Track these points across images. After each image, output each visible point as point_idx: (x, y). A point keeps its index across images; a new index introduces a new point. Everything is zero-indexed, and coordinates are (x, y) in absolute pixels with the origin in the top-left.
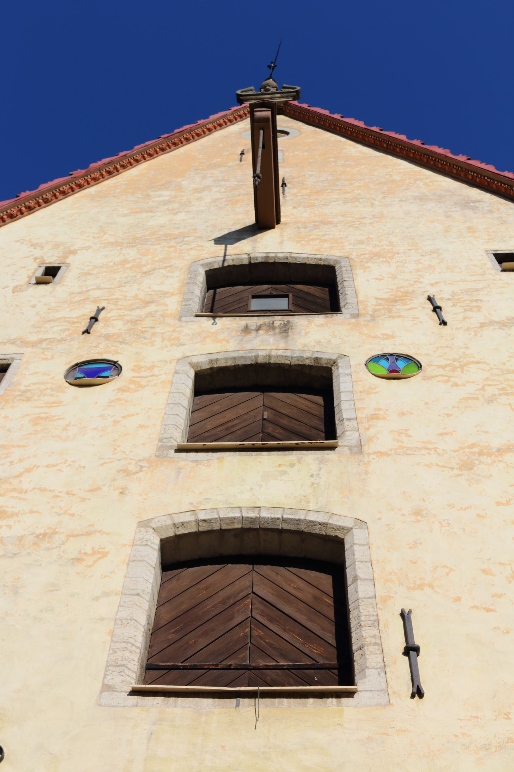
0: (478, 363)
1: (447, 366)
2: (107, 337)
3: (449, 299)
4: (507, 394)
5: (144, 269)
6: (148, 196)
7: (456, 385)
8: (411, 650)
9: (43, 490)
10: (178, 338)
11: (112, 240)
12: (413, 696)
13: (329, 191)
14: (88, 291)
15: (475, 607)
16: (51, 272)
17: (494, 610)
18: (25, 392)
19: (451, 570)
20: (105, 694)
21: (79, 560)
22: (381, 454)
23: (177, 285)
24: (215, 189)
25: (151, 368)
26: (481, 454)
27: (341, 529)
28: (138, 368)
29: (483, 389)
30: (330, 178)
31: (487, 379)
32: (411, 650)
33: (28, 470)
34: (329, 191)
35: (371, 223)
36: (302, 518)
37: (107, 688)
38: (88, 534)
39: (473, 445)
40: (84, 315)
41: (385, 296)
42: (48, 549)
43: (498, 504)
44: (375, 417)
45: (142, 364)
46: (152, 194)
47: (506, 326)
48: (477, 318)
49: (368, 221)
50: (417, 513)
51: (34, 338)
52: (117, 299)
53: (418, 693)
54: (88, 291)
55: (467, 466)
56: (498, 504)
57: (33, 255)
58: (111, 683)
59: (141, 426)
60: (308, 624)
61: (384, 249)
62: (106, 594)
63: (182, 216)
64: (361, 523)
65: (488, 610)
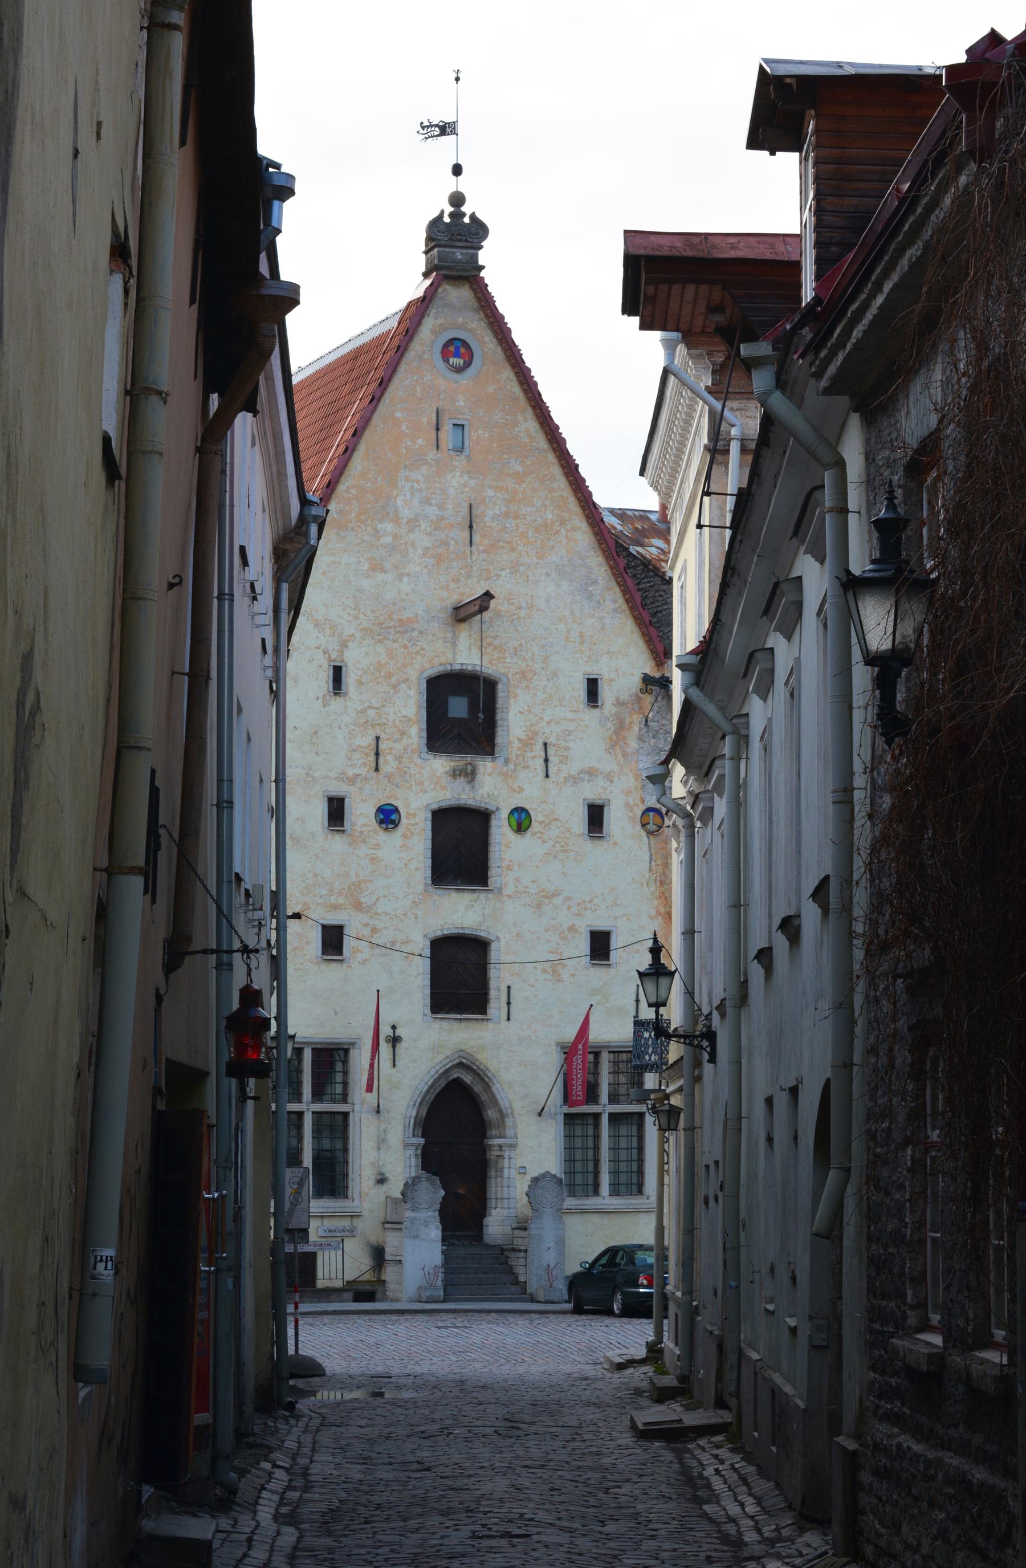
0: (556, 820)
1: (543, 821)
2: (389, 777)
3: (554, 745)
4: (563, 851)
5: (394, 680)
6: (376, 530)
7: (544, 842)
8: (509, 1003)
9: (386, 913)
10: (422, 784)
11: (365, 625)
13: (501, 544)
14: (366, 710)
16: (338, 673)
18: (361, 832)
22: (509, 896)
23: (414, 710)
24: (423, 526)
25: (415, 815)
26: (545, 897)
28: (408, 816)
29: (554, 846)
30: (504, 509)
31: (558, 836)
32: (509, 1003)
33: (378, 900)
34: (501, 544)
35: (524, 618)
37: (425, 1015)
38: (408, 942)
39: (543, 890)
40: (370, 745)
41: (523, 737)
44: (509, 868)
45: (410, 811)
46: (379, 526)
47: (575, 782)
48: (564, 774)
49: (523, 613)
50: (518, 935)
51: (351, 773)
52: (385, 724)
53: (509, 1019)
54: (366, 710)
55: (539, 906)
57: (321, 645)
59: (417, 869)
61: (528, 665)
63: (406, 586)
64: (498, 938)
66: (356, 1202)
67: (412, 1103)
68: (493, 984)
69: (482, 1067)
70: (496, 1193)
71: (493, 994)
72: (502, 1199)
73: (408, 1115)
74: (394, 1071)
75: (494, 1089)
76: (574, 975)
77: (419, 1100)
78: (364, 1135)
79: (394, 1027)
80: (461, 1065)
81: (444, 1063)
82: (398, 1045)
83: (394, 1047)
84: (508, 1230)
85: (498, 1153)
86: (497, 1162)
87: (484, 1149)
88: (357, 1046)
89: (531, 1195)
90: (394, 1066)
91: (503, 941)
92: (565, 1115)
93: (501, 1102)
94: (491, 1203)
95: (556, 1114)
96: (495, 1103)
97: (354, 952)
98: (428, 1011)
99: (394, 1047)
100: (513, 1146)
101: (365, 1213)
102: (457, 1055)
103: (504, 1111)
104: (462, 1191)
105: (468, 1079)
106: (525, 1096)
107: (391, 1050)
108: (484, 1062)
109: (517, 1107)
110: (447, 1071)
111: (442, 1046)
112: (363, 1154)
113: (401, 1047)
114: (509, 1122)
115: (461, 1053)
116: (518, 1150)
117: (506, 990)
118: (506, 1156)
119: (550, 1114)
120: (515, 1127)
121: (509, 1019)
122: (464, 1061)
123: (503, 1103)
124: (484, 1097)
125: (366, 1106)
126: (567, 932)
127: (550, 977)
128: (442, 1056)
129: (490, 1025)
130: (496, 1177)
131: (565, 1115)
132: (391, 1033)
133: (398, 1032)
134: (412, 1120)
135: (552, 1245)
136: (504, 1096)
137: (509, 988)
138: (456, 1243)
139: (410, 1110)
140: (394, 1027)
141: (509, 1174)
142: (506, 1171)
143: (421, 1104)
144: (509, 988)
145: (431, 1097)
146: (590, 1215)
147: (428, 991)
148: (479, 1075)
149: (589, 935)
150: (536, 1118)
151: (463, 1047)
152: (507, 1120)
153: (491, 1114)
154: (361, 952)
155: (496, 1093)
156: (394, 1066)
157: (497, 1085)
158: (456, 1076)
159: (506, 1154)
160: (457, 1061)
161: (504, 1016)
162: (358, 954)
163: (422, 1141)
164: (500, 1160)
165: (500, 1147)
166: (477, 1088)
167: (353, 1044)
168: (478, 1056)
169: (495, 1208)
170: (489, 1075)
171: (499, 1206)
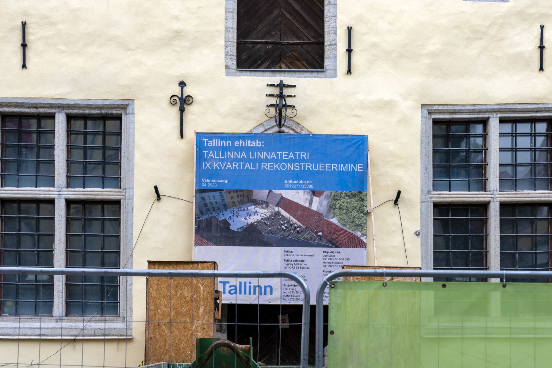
8: (349, 51)
32: (349, 51)
53: (349, 72)
79: (182, 84)
83: (182, 110)
88: (129, 110)
92: (436, 205)
99: (182, 110)
121: (349, 72)
131: (436, 205)
132: (177, 90)
133: (188, 91)
137: (350, 30)
140: (182, 84)
144: (350, 30)
167: (125, 107)
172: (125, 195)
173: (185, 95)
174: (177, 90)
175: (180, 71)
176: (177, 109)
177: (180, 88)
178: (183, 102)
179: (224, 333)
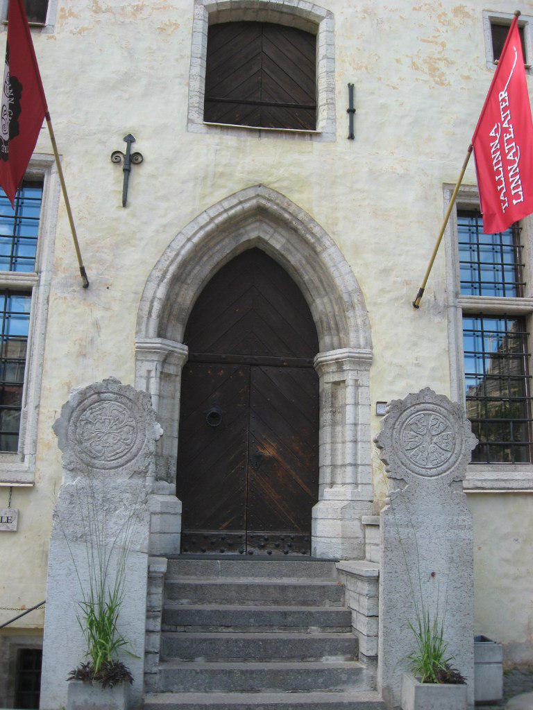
8: (351, 111)
12: (349, 138)
15: (388, 85)
17: (397, 89)
19: (379, 57)
20: (190, 125)
21: (162, 29)
27: (319, 16)
32: (351, 111)
36: (296, 6)
37: (190, 121)
42: (142, 19)
43: (414, 9)
53: (351, 137)
56: (414, 9)
58: (192, 117)
60: (295, 78)
62: (182, 57)
64: (330, 14)
65: (394, 88)
66: (26, 464)
67: (158, 274)
68: (322, 83)
69: (301, 216)
70: (333, 455)
71: (322, 98)
72: (343, 465)
73: (149, 294)
74: (124, 213)
75: (325, 257)
76: (468, 78)
77: (172, 269)
78: (53, 328)
79: (130, 139)
80: (261, 213)
81: (226, 205)
82: (134, 169)
83: (127, 171)
84: (355, 528)
85: (336, 378)
86: (334, 396)
87: (311, 375)
89: (385, 442)
90: (125, 204)
91: (339, 19)
93: (338, 281)
94: (325, 475)
95: (447, 307)
96: (328, 285)
97: (63, 17)
98: (198, 117)
99: (127, 171)
100: (364, 362)
101: (43, 486)
102: (252, 193)
103: (346, 298)
104: (269, 452)
105: (277, 241)
106: (386, 272)
107: (122, 178)
108: (305, 206)
109: (371, 289)
110: (232, 225)
111: (222, 175)
112: (47, 366)
113: (140, 175)
114: (354, 318)
115: (260, 191)
116: (373, 371)
117: (347, 90)
118: (350, 382)
119: (436, 306)
120: (367, 326)
121: (351, 137)
122: (269, 205)
123: (343, 282)
124: (308, 276)
125: (61, 275)
126: (450, 16)
127: (426, 77)
128: (223, 193)
129: (316, 146)
130: (334, 424)
132: (123, 147)
133: (136, 148)
134: (157, 306)
135: (440, 565)
136: (344, 269)
137: (351, 88)
138: (257, 551)
139: (152, 285)
140: (130, 139)
141: (356, 416)
142: (349, 410)
143: (177, 280)
144: (351, 88)
145: (204, 270)
146: (521, 500)
147: (199, 85)
148: (295, 230)
149: (488, 25)
150: (411, 312)
151: (265, 180)
152: (350, 314)
153: (320, 306)
154: (76, 17)
155: (329, 264)
156: (125, 204)
157: (332, 250)
158: (253, 235)
159: (349, 377)
160: (254, 202)
161: (346, 133)
162: (71, 20)
163: (183, 350)
164: (340, 394)
165: (339, 363)
166: (295, 259)
168: (295, 197)
169: (332, 484)
170: (316, 230)
171: (339, 480)
172: (39, 281)
173: (133, 151)
174: (123, 147)
175: (130, 125)
176: (121, 168)
177: (126, 144)
178: (129, 161)
179: (171, 482)
